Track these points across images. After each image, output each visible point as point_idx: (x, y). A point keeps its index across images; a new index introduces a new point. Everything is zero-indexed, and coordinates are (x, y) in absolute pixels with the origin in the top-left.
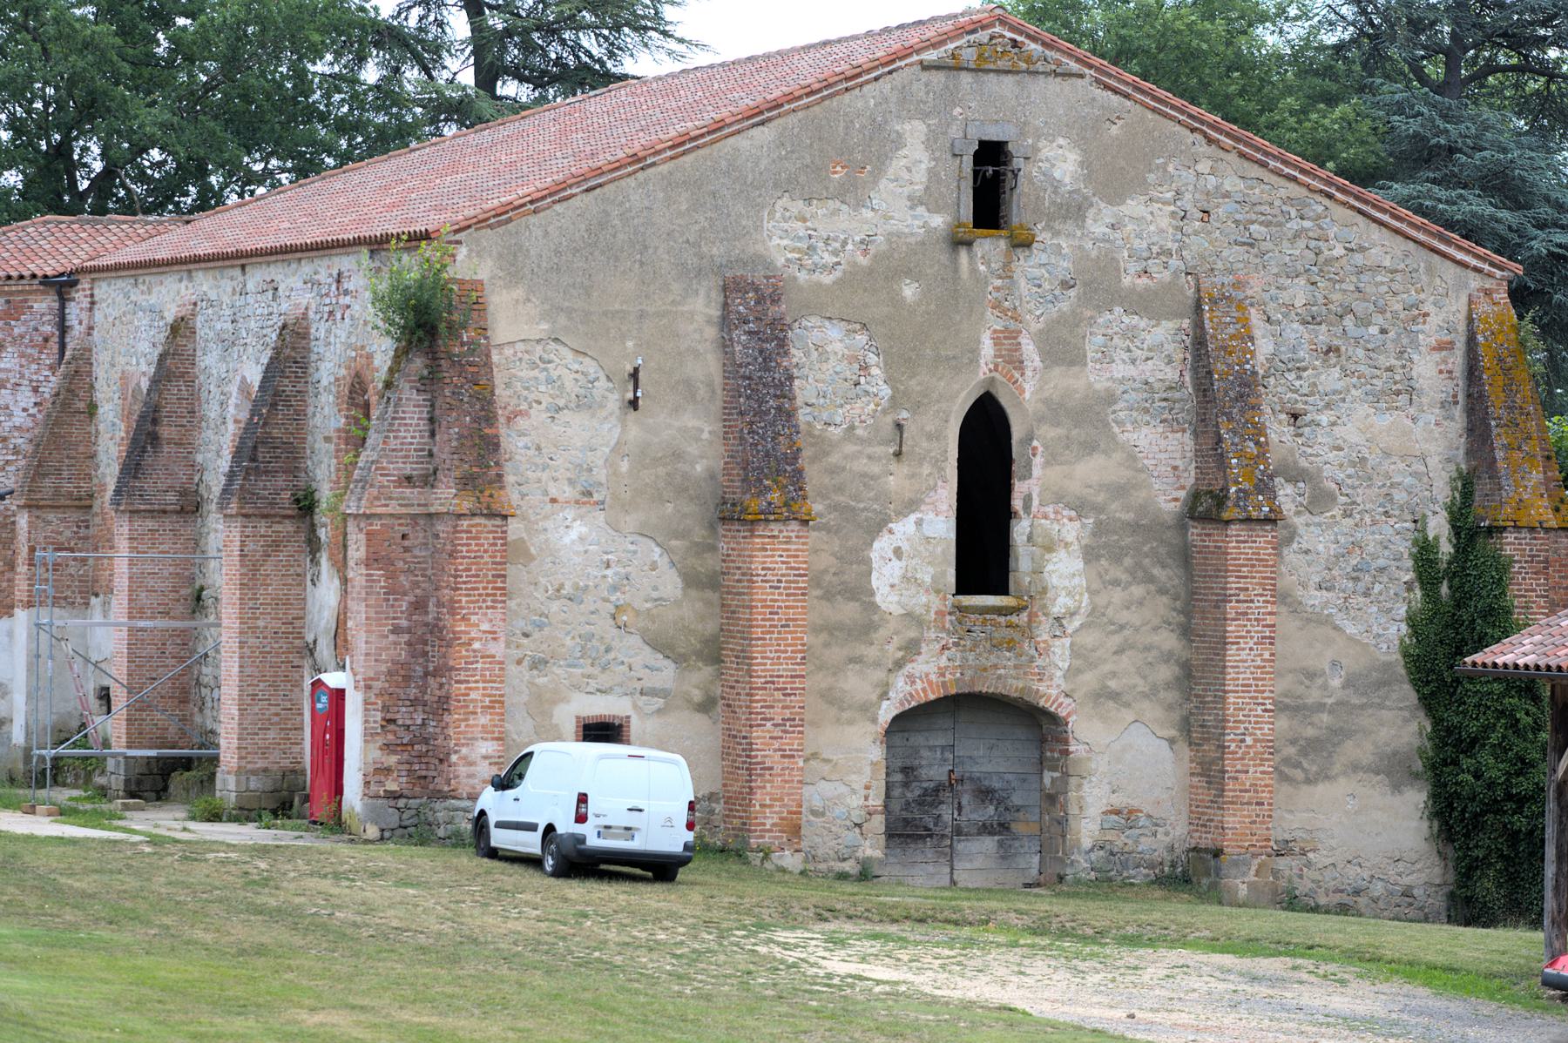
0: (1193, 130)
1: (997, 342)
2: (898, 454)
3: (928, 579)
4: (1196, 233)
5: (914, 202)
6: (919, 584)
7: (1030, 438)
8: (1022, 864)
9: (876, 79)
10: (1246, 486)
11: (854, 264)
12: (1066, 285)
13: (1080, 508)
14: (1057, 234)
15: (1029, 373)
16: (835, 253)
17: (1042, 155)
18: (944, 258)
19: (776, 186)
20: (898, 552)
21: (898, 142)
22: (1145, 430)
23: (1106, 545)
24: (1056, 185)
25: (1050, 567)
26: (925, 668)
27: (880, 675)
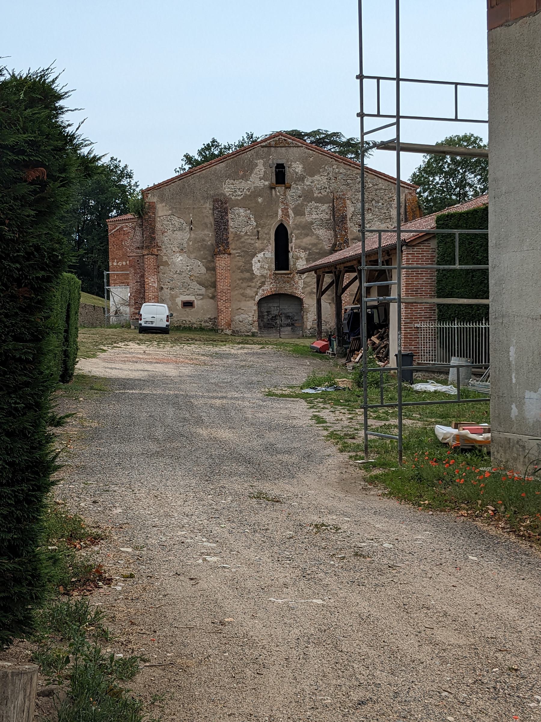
0: (332, 158)
1: (282, 211)
2: (258, 238)
3: (267, 267)
4: (333, 183)
5: (261, 179)
6: (265, 268)
7: (292, 233)
8: (297, 333)
9: (250, 150)
10: (341, 242)
11: (246, 194)
12: (300, 197)
13: (305, 249)
14: (297, 185)
15: (291, 218)
16: (241, 192)
17: (292, 166)
18: (268, 192)
19: (226, 177)
20: (259, 261)
21: (256, 165)
22: (321, 230)
23: (311, 258)
24: (297, 173)
25: (297, 263)
26: (267, 288)
27: (256, 290)
